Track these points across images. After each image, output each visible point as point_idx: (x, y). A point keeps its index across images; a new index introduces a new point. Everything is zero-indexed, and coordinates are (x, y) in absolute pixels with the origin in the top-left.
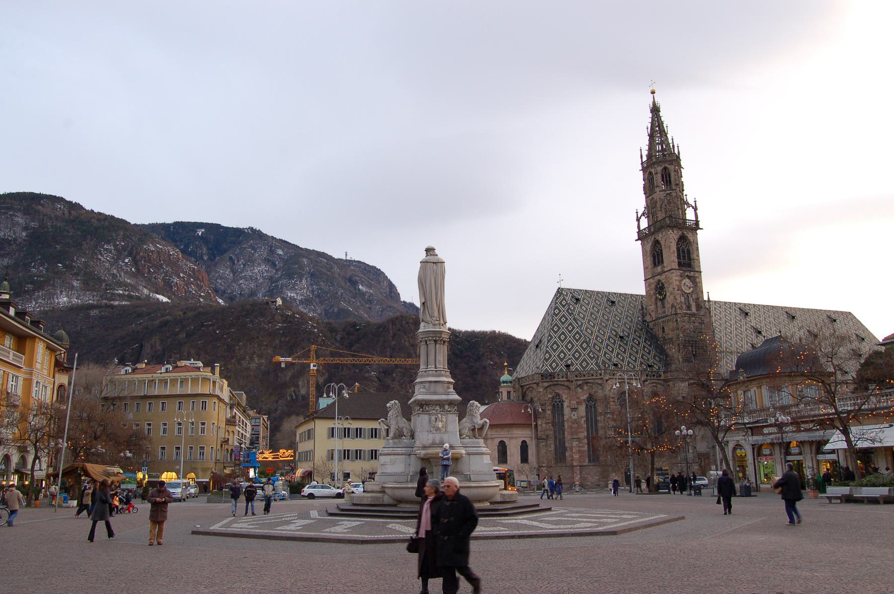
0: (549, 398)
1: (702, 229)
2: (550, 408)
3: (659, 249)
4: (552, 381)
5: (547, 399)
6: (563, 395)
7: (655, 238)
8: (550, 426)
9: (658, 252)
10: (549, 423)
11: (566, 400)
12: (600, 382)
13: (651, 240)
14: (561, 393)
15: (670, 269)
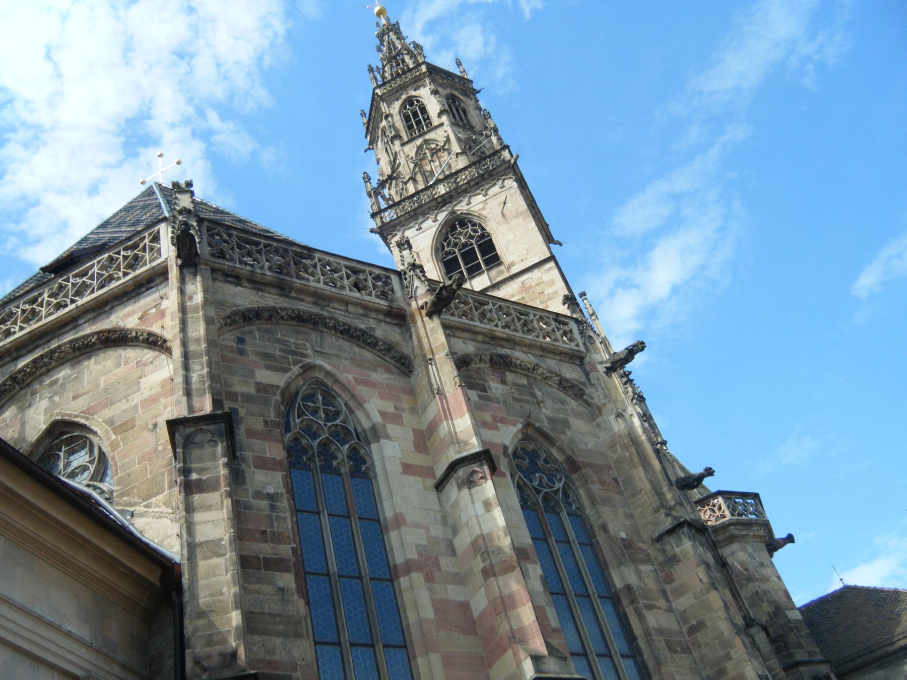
0: (263, 388)
1: (561, 245)
2: (276, 451)
3: (471, 237)
4: (283, 289)
5: (252, 390)
6: (362, 391)
7: (453, 212)
8: (282, 590)
9: (465, 245)
10: (275, 564)
11: (392, 429)
12: (570, 372)
13: (435, 221)
14: (347, 377)
15: (537, 260)
